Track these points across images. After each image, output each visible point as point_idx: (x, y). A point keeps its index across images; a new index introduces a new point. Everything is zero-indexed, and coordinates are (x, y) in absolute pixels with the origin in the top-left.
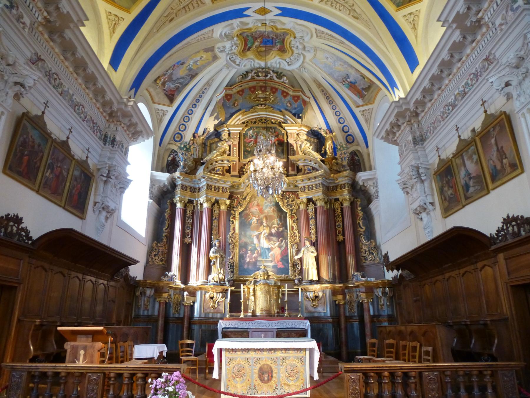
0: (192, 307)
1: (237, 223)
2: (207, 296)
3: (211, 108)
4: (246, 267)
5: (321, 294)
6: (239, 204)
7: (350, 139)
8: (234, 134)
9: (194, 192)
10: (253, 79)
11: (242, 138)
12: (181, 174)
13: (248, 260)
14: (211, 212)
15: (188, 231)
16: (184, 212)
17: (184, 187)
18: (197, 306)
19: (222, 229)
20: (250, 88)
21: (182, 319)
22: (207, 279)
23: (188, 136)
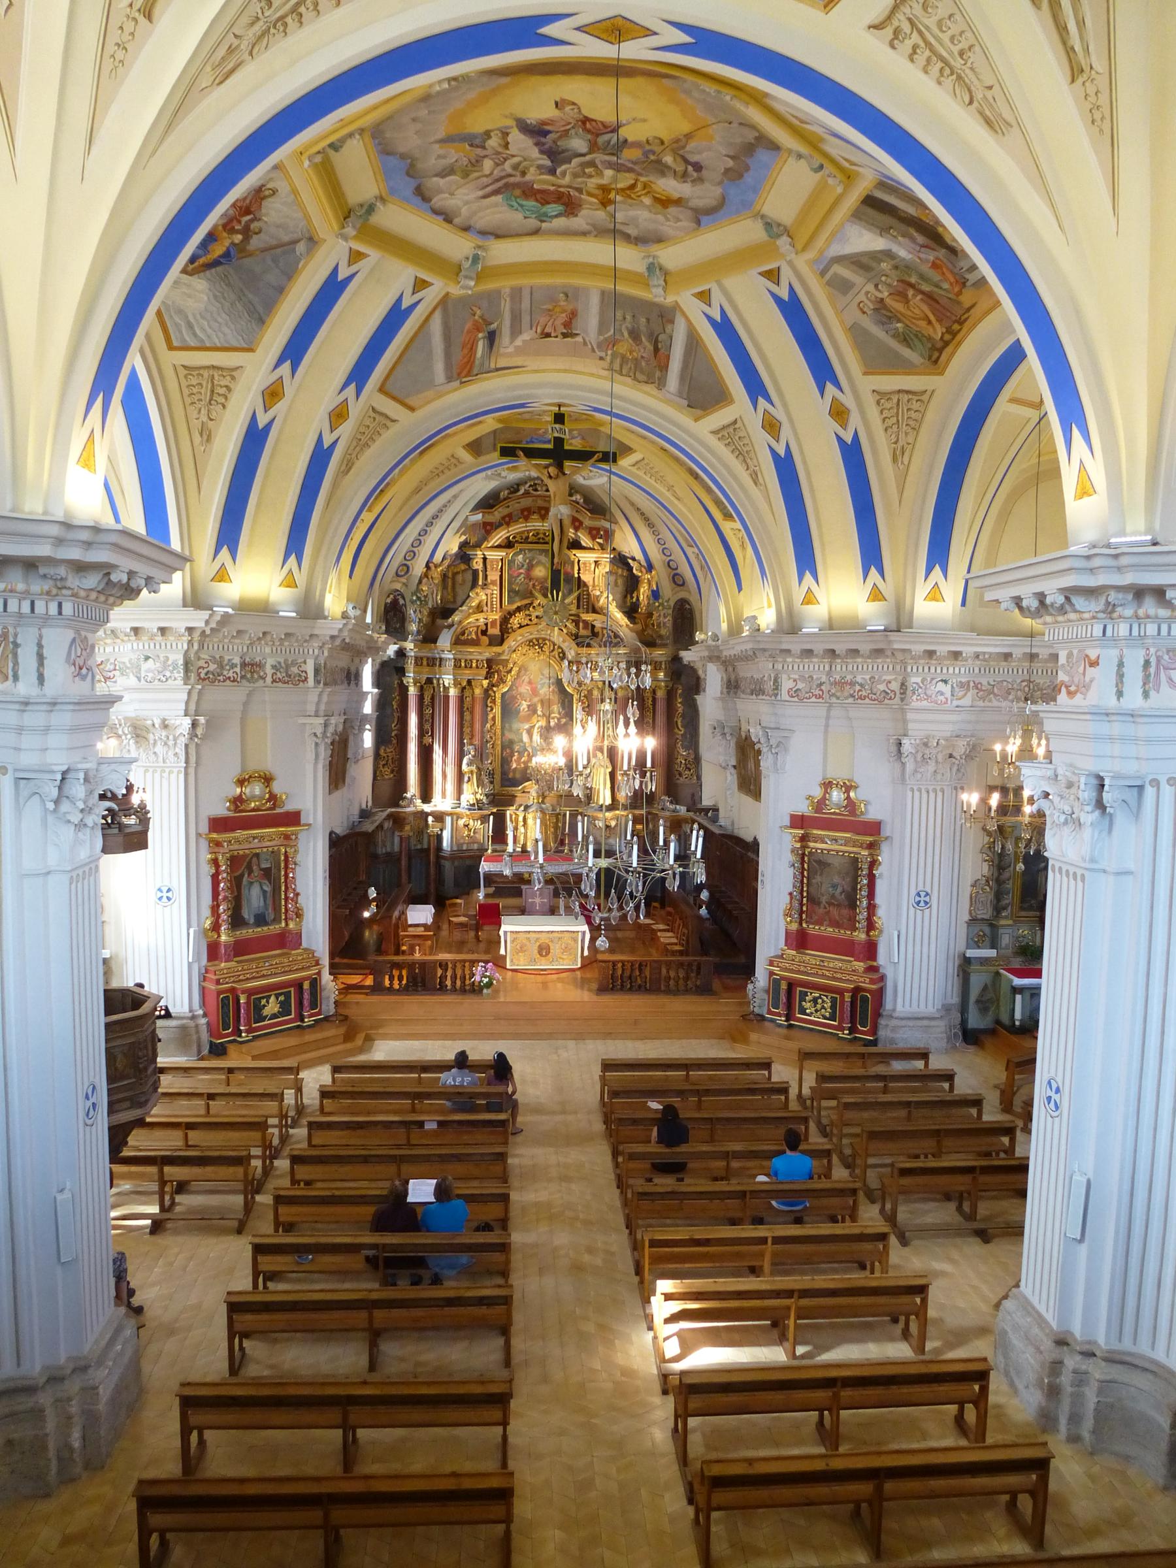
0: (439, 838)
1: (498, 710)
2: (461, 822)
3: (456, 524)
4: (511, 776)
5: (613, 823)
6: (502, 681)
7: (677, 580)
8: (492, 561)
9: (434, 665)
10: (527, 493)
11: (506, 568)
12: (415, 646)
13: (514, 766)
14: (461, 699)
15: (427, 726)
16: (421, 698)
17: (418, 661)
18: (446, 835)
19: (477, 726)
20: (523, 511)
21: (428, 850)
22: (459, 799)
23: (418, 568)
